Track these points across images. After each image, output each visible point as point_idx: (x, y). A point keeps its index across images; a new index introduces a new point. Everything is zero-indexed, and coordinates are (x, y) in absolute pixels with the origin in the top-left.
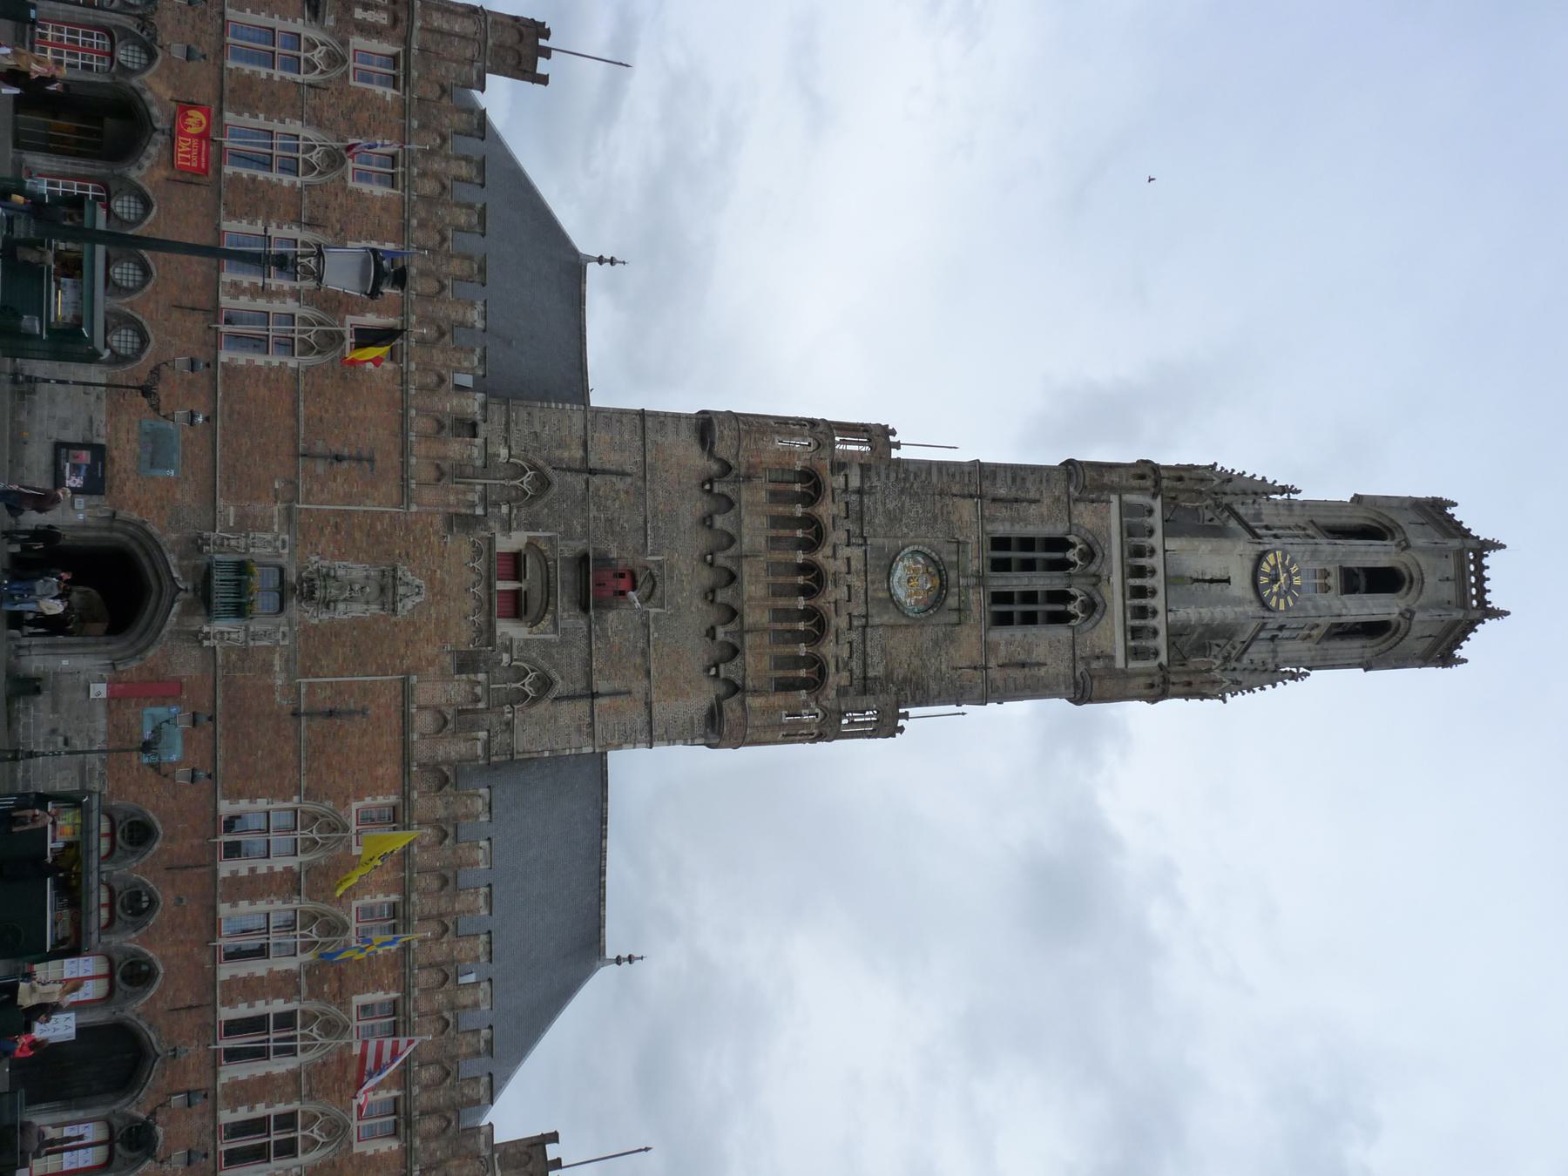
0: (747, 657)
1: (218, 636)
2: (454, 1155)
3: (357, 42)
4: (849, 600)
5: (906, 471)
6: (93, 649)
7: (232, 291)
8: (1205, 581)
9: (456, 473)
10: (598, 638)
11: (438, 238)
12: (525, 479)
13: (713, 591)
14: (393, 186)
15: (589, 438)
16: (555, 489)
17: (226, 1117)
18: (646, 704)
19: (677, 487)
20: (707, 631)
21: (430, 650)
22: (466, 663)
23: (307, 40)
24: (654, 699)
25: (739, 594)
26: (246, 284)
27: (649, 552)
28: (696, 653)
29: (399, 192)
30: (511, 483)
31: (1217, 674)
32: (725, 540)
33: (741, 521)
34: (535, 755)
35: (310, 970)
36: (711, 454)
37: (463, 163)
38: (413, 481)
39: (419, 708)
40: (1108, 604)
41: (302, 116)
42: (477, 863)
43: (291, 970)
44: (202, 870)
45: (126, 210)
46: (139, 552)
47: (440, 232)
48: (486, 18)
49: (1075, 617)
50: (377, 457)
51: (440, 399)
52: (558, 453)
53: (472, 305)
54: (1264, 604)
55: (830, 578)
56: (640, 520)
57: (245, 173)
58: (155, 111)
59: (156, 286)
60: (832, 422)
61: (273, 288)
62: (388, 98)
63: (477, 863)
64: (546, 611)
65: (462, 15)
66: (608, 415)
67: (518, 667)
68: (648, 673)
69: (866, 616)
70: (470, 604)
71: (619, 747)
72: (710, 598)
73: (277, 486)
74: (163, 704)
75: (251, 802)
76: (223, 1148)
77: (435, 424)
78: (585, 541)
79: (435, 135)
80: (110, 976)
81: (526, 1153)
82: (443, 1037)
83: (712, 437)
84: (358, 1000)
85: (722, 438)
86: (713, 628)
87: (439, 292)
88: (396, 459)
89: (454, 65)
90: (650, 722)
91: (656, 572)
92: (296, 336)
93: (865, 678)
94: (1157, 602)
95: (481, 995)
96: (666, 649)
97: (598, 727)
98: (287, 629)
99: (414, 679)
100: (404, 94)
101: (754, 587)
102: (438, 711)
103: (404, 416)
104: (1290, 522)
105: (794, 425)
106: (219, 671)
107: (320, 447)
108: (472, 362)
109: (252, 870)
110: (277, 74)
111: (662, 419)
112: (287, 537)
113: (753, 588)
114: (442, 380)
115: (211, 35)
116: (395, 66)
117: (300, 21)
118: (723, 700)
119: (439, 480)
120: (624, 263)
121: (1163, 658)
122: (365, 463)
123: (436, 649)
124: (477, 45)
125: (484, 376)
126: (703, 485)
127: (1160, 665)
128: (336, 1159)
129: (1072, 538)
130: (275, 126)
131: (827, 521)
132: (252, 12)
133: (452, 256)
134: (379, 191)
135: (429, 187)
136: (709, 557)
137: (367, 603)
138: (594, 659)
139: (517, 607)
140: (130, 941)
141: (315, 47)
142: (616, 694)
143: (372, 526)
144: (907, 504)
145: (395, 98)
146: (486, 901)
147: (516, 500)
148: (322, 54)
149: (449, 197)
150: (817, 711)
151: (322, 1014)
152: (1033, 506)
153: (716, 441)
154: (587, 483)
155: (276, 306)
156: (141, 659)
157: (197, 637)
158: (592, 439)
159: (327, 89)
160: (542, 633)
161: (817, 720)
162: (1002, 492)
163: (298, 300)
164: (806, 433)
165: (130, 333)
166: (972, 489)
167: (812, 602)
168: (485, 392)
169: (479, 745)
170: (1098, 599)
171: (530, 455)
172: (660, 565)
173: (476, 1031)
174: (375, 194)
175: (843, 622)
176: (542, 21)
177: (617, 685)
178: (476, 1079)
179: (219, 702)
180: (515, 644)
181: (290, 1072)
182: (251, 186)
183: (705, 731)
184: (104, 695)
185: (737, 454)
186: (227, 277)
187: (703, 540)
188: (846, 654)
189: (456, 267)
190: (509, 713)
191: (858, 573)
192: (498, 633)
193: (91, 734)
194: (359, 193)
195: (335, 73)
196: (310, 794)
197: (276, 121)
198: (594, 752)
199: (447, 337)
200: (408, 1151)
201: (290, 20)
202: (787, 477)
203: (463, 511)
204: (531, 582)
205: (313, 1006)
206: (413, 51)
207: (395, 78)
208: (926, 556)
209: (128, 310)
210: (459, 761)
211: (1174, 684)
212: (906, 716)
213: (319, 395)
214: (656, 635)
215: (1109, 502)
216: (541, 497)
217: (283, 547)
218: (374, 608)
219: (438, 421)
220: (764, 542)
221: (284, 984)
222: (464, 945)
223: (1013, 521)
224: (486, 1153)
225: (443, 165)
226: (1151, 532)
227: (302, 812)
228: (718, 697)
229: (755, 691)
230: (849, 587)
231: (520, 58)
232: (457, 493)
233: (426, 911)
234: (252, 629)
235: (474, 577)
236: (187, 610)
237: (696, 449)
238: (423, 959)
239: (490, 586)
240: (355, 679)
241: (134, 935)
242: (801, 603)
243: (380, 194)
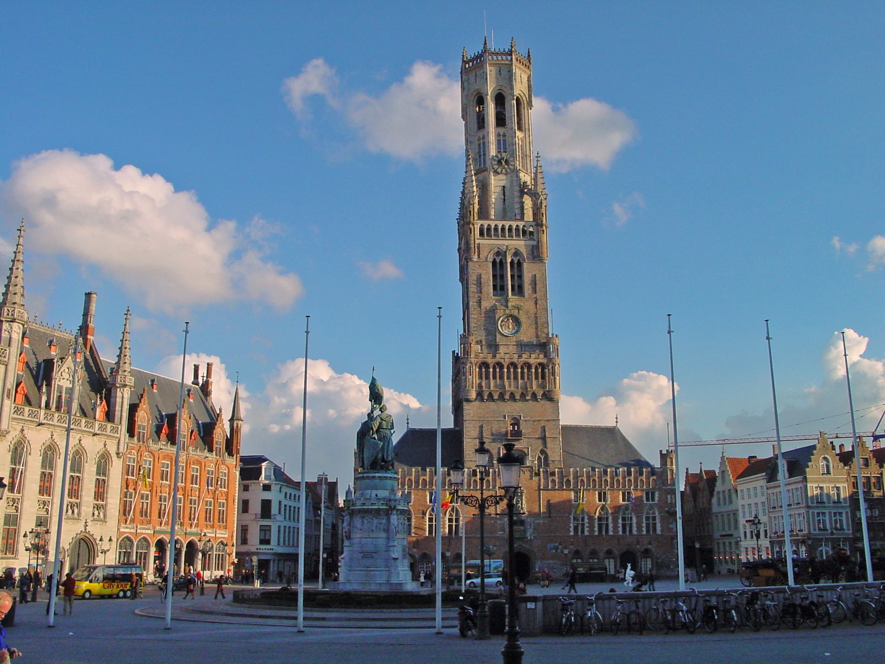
5: (474, 327)
8: (504, 199)
17: (644, 533)
31: (539, 201)
40: (515, 247)
49: (519, 260)
54: (513, 171)
55: (511, 360)
69: (521, 345)
76: (651, 533)
80: (609, 558)
93: (540, 345)
94: (514, 224)
104: (477, 143)
121: (534, 224)
127: (536, 225)
129: (491, 260)
131: (494, 361)
134: (413, 497)
152: (482, 276)
167: (519, 366)
172: (508, 416)
187: (501, 403)
191: (508, 348)
196: (570, 514)
200: (659, 489)
205: (621, 513)
208: (502, 322)
211: (542, 221)
213: (468, 511)
215: (479, 244)
218: (523, 497)
223: (489, 285)
224: (662, 469)
226: (489, 225)
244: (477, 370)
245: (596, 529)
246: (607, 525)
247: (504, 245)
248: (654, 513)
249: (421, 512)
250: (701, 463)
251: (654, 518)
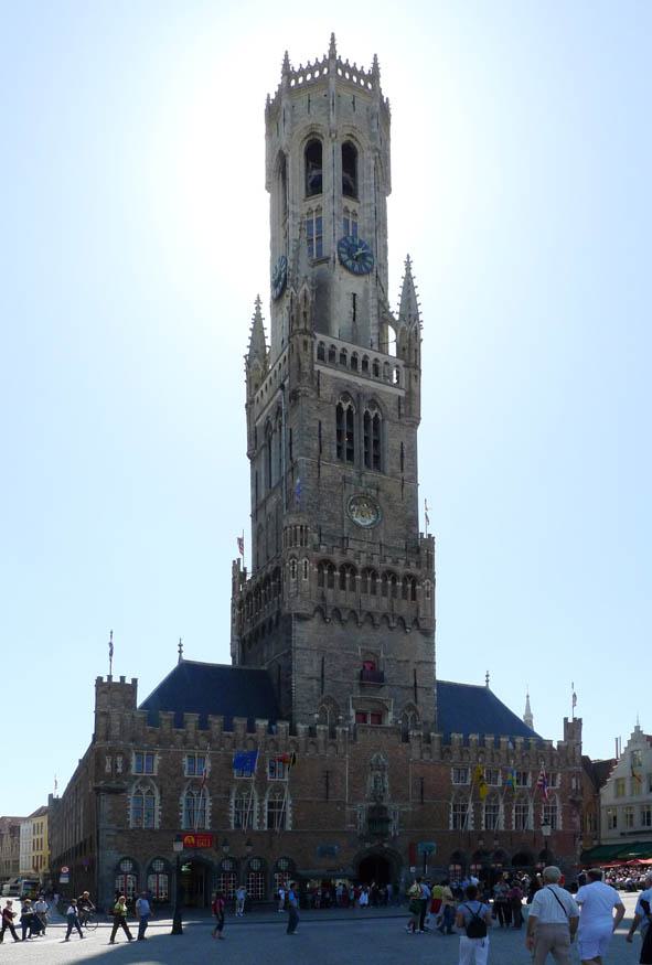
16: (331, 694)
21: (401, 753)
22: (406, 738)
39: (422, 758)
43: (506, 807)
49: (376, 415)
68: (407, 661)
102: (422, 753)
121: (401, 363)
127: (404, 366)
139: (379, 717)
144: (323, 507)
152: (323, 426)
162: (316, 445)
166: (315, 465)
167: (380, 574)
170: (370, 398)
177: (411, 674)
181: (534, 808)
191: (360, 545)
196: (450, 800)
204: (368, 708)
208: (351, 503)
212: (430, 535)
218: (386, 773)
242: (379, 581)
244: (316, 570)
247: (356, 384)
248: (554, 802)
251: (554, 809)
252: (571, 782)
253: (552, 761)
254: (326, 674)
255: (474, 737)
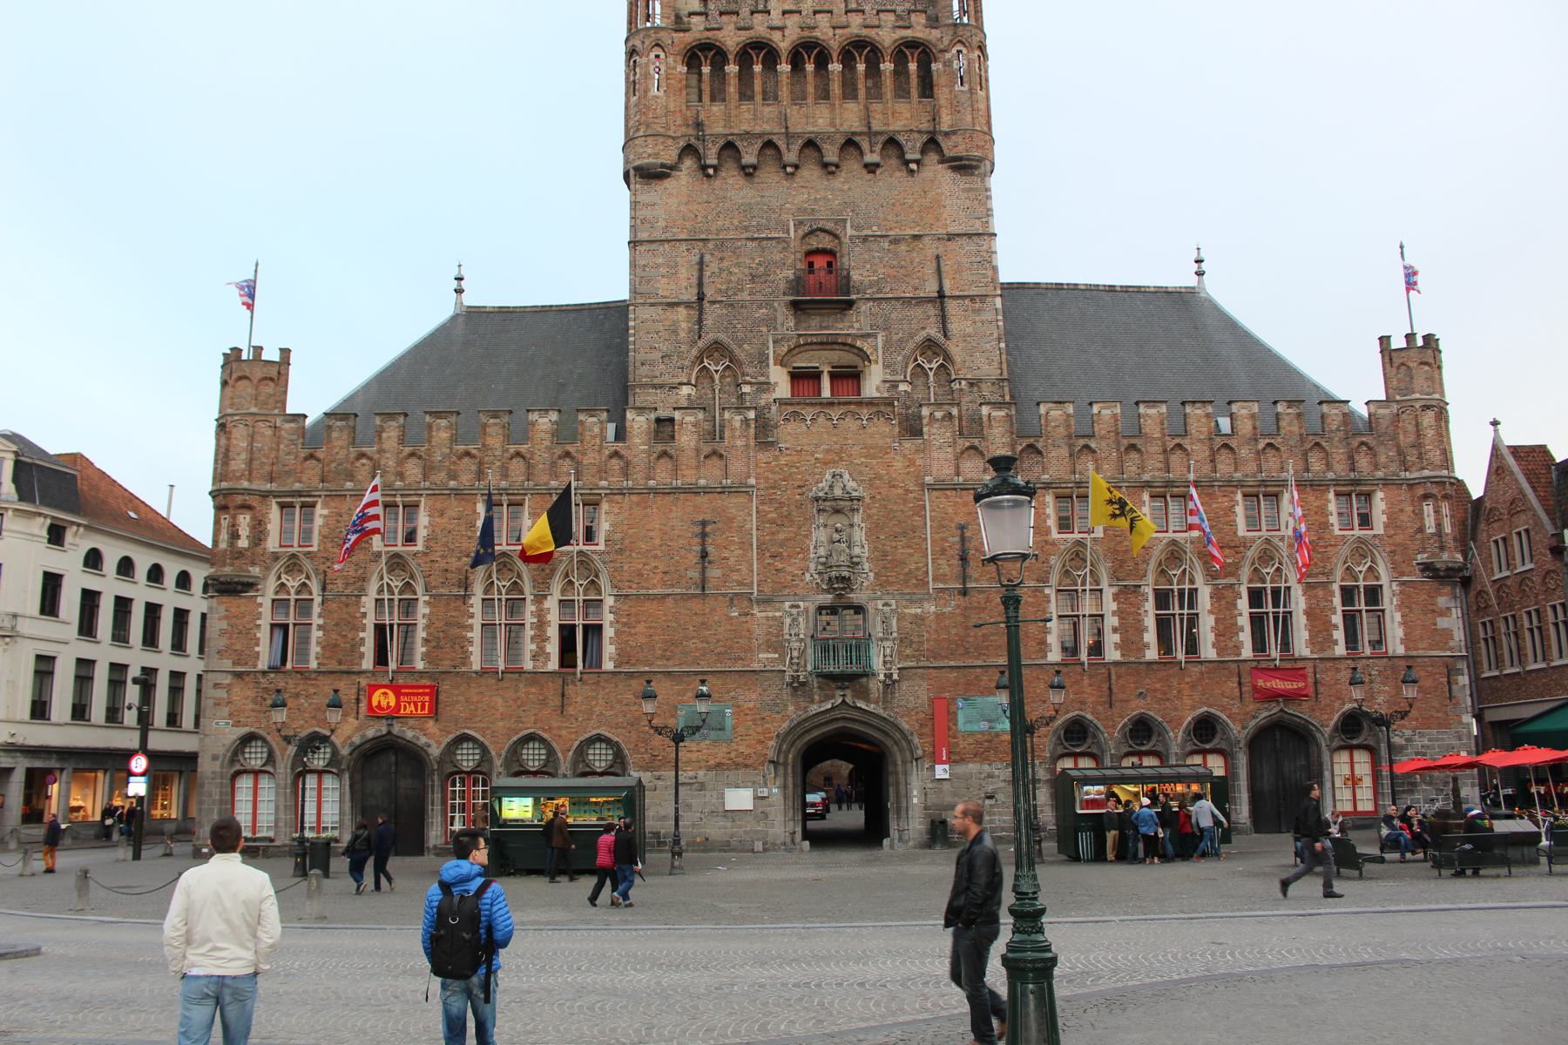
0: (897, 129)
1: (888, 666)
2: (1394, 438)
3: (272, 544)
4: (830, 12)
6: (901, 776)
7: (542, 659)
9: (713, 435)
10: (881, 293)
11: (466, 460)
12: (713, 368)
13: (825, 165)
14: (417, 506)
15: (664, 300)
16: (722, 337)
18: (949, 240)
19: (713, 206)
20: (869, 172)
21: (899, 464)
22: (912, 428)
23: (277, 593)
24: (945, 232)
25: (829, 137)
26: (534, 647)
27: (781, 235)
28: (892, 182)
29: (423, 499)
30: (717, 381)
32: (769, 152)
33: (748, 133)
34: (1004, 357)
35: (1211, 575)
36: (673, 168)
37: (384, 435)
38: (724, 481)
39: (958, 474)
41: (357, 596)
42: (1114, 416)
43: (1211, 593)
44: (1113, 677)
45: (471, 757)
46: (807, 738)
47: (460, 458)
48: (229, 415)
50: (701, 519)
51: (635, 456)
52: (682, 334)
53: (533, 424)
55: (806, 33)
56: (749, 244)
57: (420, 650)
58: (371, 733)
59: (544, 730)
60: (629, 30)
61: (535, 620)
62: (326, 512)
63: (1114, 416)
64: (851, 346)
65: (228, 439)
66: (638, 280)
67: (912, 374)
68: (916, 237)
70: (850, 424)
71: (995, 269)
72: (834, 169)
73: (736, 614)
74: (955, 713)
75: (1049, 633)
76: (1368, 651)
77: (662, 461)
78: (776, 304)
79: (358, 464)
81: (1398, 368)
82: (1282, 449)
83: (653, 164)
84: (1242, 530)
85: (656, 155)
86: (866, 166)
87: (523, 457)
88: (702, 500)
89: (282, 446)
90: (970, 236)
91: (807, 229)
92: (582, 598)
95: (1244, 412)
96: (890, 218)
97: (974, 291)
98: (880, 604)
99: (928, 479)
100: (320, 496)
101: (819, 119)
102: (959, 457)
103: (655, 491)
105: (635, 74)
106: (921, 664)
107: (694, 574)
108: (595, 424)
109: (1115, 630)
110: (316, 620)
111: (638, 221)
112: (787, 604)
113: (820, 121)
114: (616, 454)
115: (287, 683)
116: (291, 506)
117: (259, 600)
118: (944, 156)
119: (721, 456)
120: (460, 266)
122: (708, 529)
123: (898, 458)
124: (260, 423)
125: (608, 411)
126: (708, 176)
128: (1388, 549)
130: (370, 622)
131: (743, 37)
132: (258, 645)
133: (484, 445)
134: (423, 520)
135: (413, 470)
136: (789, 170)
137: (852, 526)
138: (903, 295)
139: (849, 377)
140: (1176, 737)
141: (283, 585)
142: (939, 270)
143: (772, 522)
145: (325, 505)
146: (1154, 407)
147: (735, 376)
148: (290, 578)
149: (423, 449)
150: (954, 51)
151: (1253, 564)
153: (659, 161)
154: (714, 302)
155: (554, 619)
156: (912, 734)
157: (889, 685)
158: (666, 297)
159: (325, 572)
160: (876, 350)
161: (965, 51)
163: (545, 597)
164: (644, 60)
165: (591, 751)
168: (625, 410)
169: (994, 414)
171: (687, 363)
173: (1278, 416)
174: (427, 524)
175: (856, 20)
176: (222, 357)
177: (930, 269)
178: (1323, 416)
179: (952, 663)
180: (889, 378)
182: (434, 644)
183: (978, 176)
184: (947, 767)
185: (674, 138)
186: (528, 665)
187: (769, 176)
188: (891, 17)
189: (495, 440)
190: (960, 383)
192: (878, 395)
193: (983, 776)
194: (428, 540)
195: (308, 565)
196: (1044, 580)
197: (364, 621)
198: (1001, 296)
199: (570, 448)
200: (1386, 483)
201: (260, 610)
202: (694, 82)
203: (752, 431)
204: (822, 361)
205: (1245, 573)
206: (273, 489)
207: (303, 506)
209: (571, 753)
210: (1012, 433)
213: (640, 575)
214: (875, 228)
216: (731, 352)
217: (798, 607)
218: (857, 519)
219: (659, 458)
220: (770, 109)
221: (1223, 599)
222: (1193, 427)
224: (1395, 408)
225: (388, 455)
227: (1060, 585)
228: (942, 162)
229: (934, 120)
230: (815, 13)
231: (265, 379)
232: (733, 437)
233: (1160, 465)
234: (881, 635)
235: (821, 419)
236: (864, 694)
237: (667, 183)
238: (1207, 469)
239: (830, 404)
240: (929, 536)
241: (1171, 734)
242: (835, 67)
243: (427, 519)
245: (1150, 637)
246: (1193, 621)
249: (454, 577)
250: (1495, 423)
251: (1373, 594)
252: (1419, 515)
253: (1351, 458)
254: (709, 292)
255: (1105, 413)
